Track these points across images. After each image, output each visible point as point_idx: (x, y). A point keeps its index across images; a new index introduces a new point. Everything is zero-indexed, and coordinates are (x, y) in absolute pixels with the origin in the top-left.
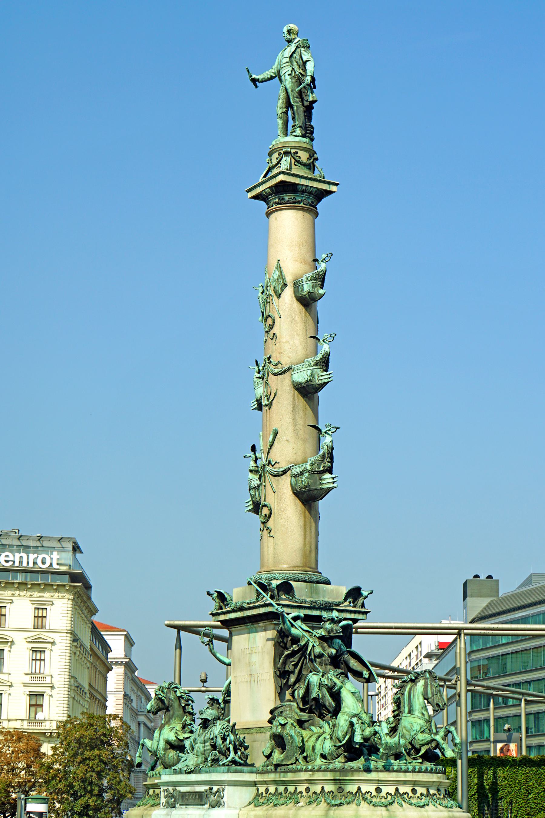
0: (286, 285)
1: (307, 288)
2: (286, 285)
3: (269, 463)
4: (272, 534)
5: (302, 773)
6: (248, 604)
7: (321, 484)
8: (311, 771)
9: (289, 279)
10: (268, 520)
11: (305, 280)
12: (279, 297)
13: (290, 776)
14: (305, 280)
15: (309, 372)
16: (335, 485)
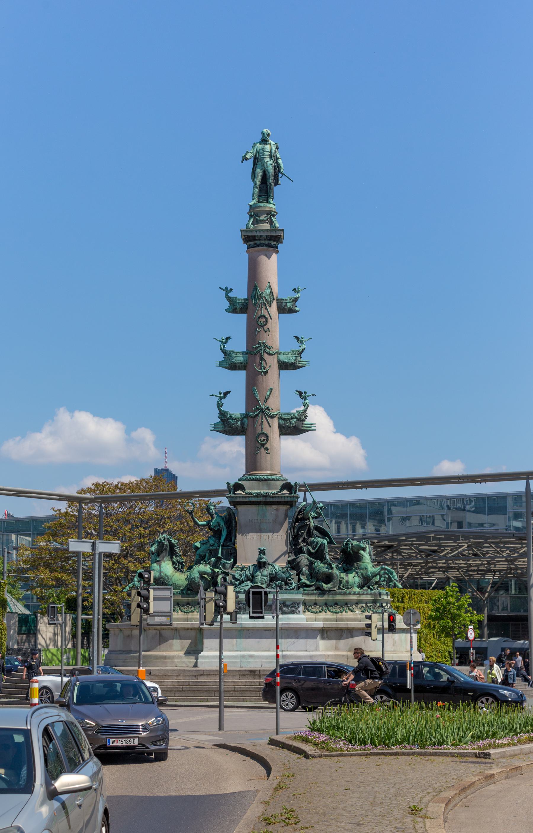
0: (274, 299)
1: (289, 305)
2: (274, 299)
3: (268, 409)
4: (269, 452)
5: (351, 595)
6: (273, 494)
7: (302, 427)
8: (358, 594)
9: (275, 297)
10: (266, 443)
11: (288, 300)
12: (270, 306)
13: (339, 597)
14: (288, 300)
15: (294, 358)
16: (312, 428)
